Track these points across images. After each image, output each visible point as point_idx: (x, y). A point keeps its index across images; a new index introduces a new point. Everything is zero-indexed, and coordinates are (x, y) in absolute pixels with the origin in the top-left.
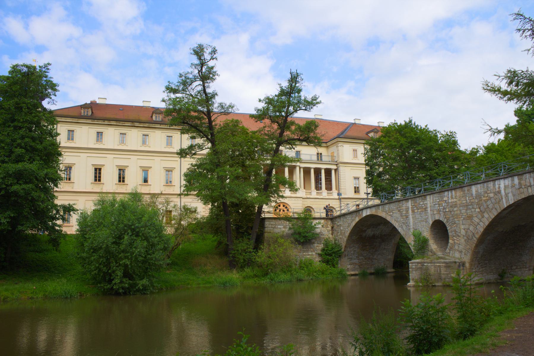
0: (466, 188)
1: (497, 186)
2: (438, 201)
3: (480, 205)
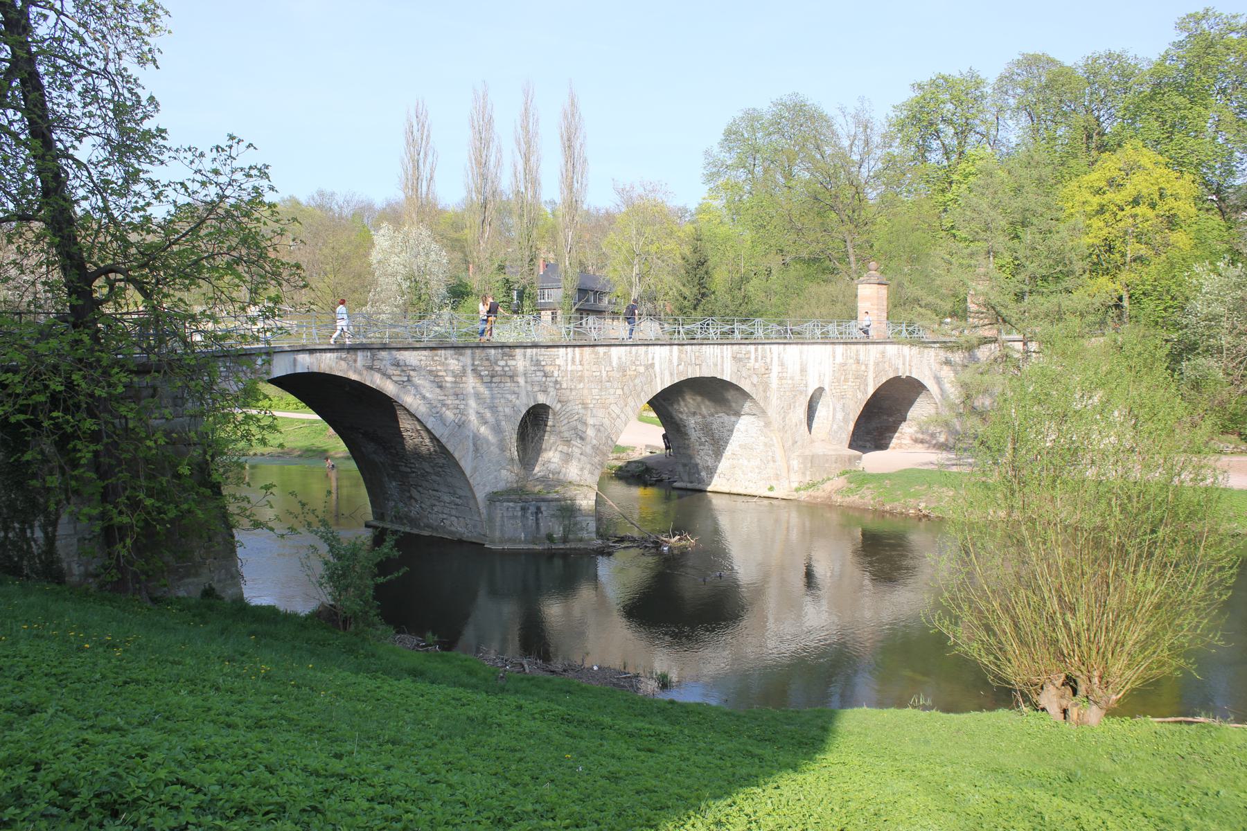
1: (650, 356)
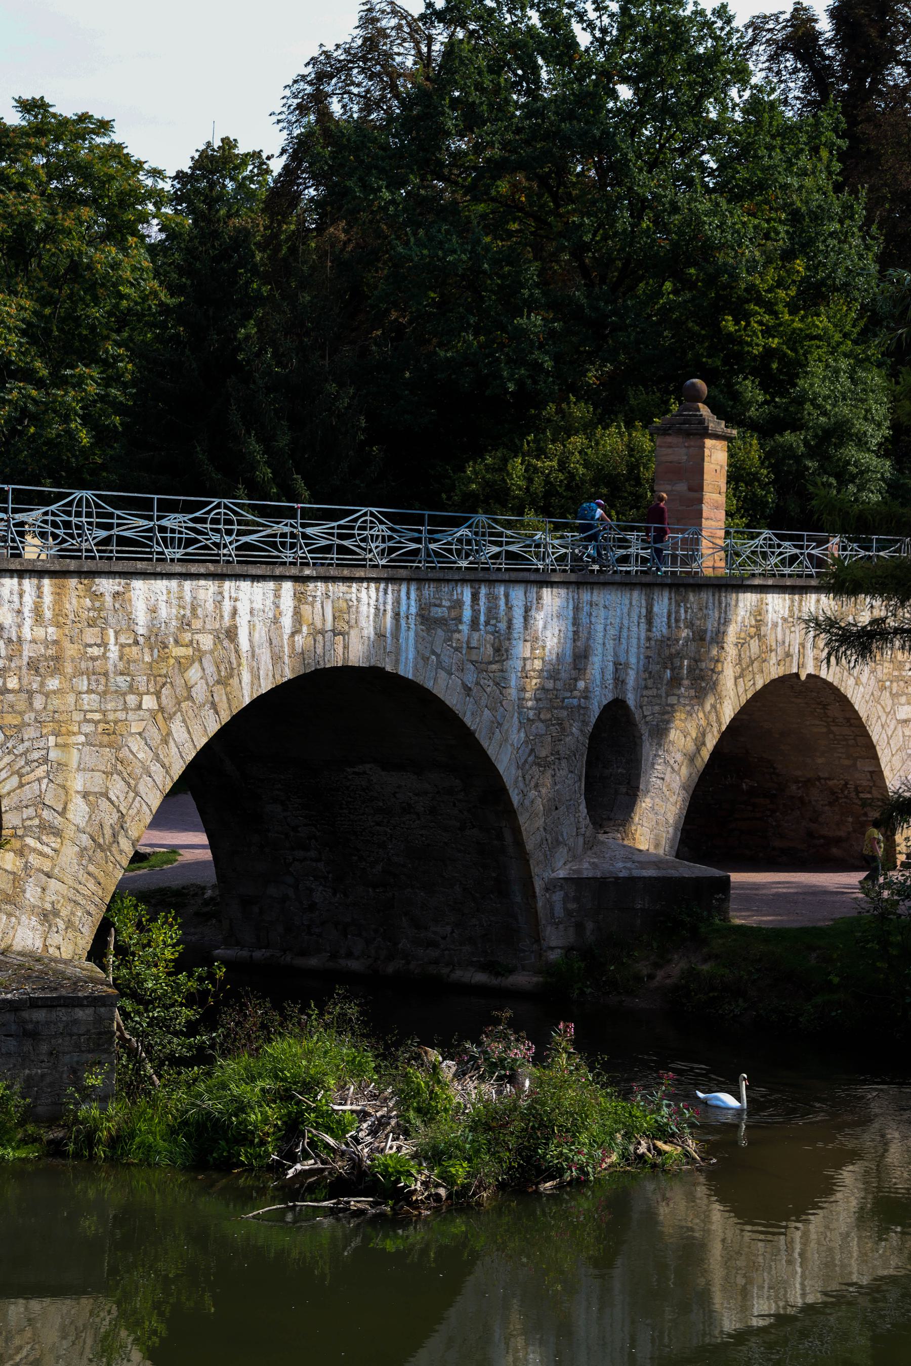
1: (227, 606)
3: (161, 680)
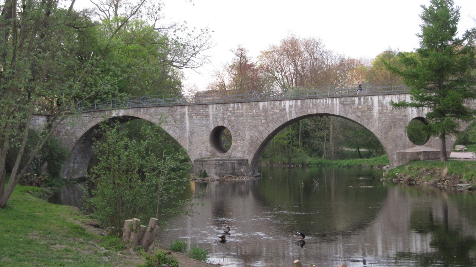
0: (254, 103)
1: (283, 105)
2: (222, 110)
